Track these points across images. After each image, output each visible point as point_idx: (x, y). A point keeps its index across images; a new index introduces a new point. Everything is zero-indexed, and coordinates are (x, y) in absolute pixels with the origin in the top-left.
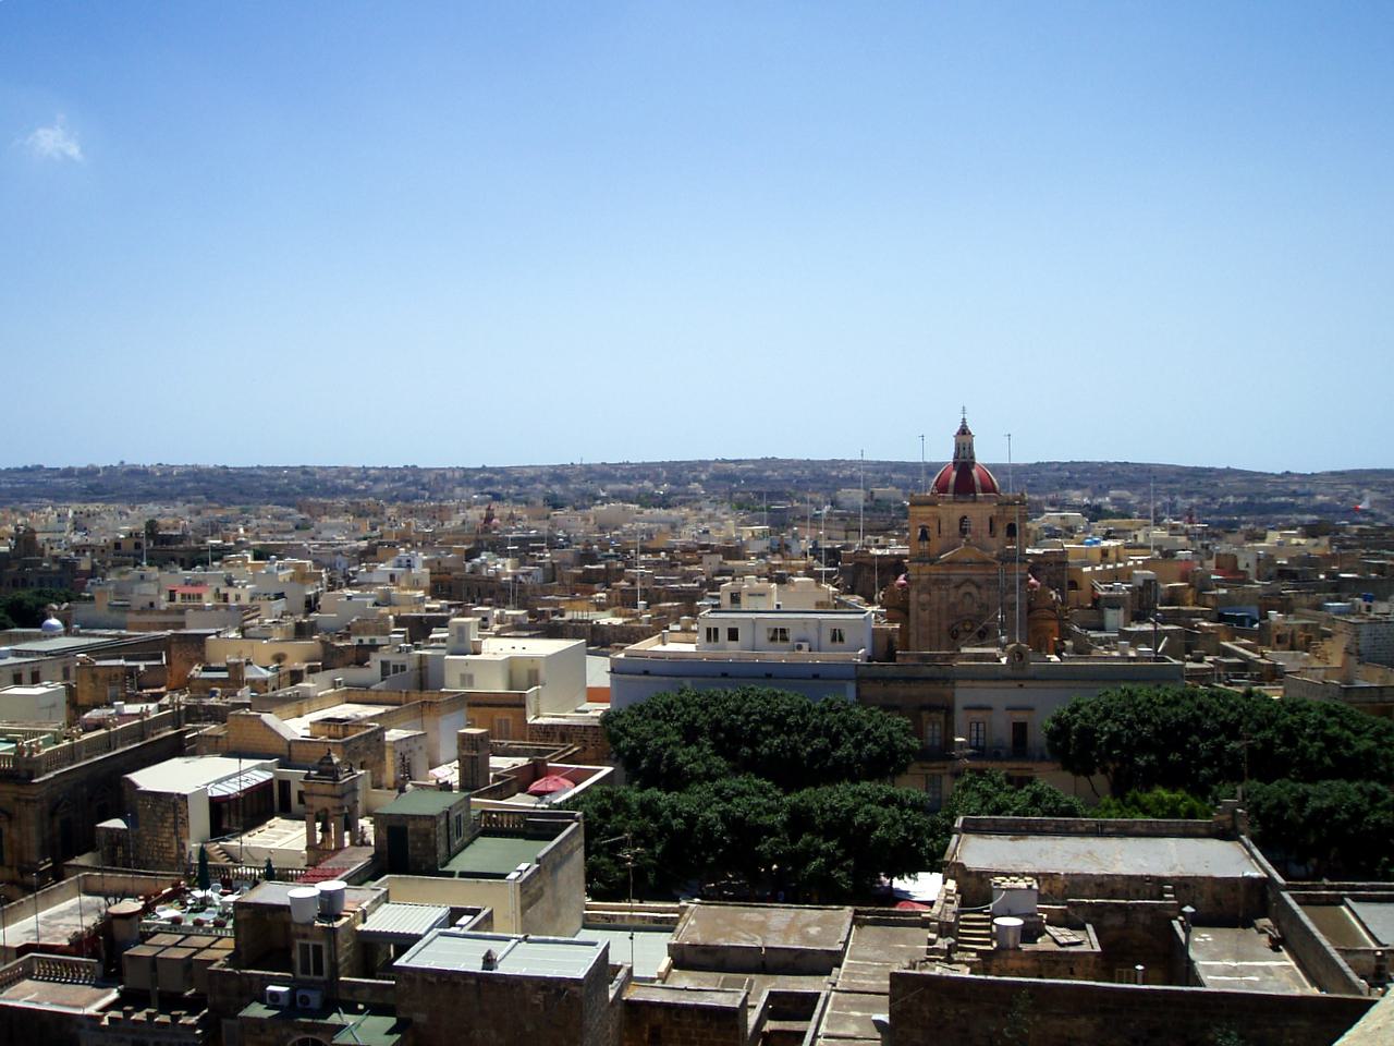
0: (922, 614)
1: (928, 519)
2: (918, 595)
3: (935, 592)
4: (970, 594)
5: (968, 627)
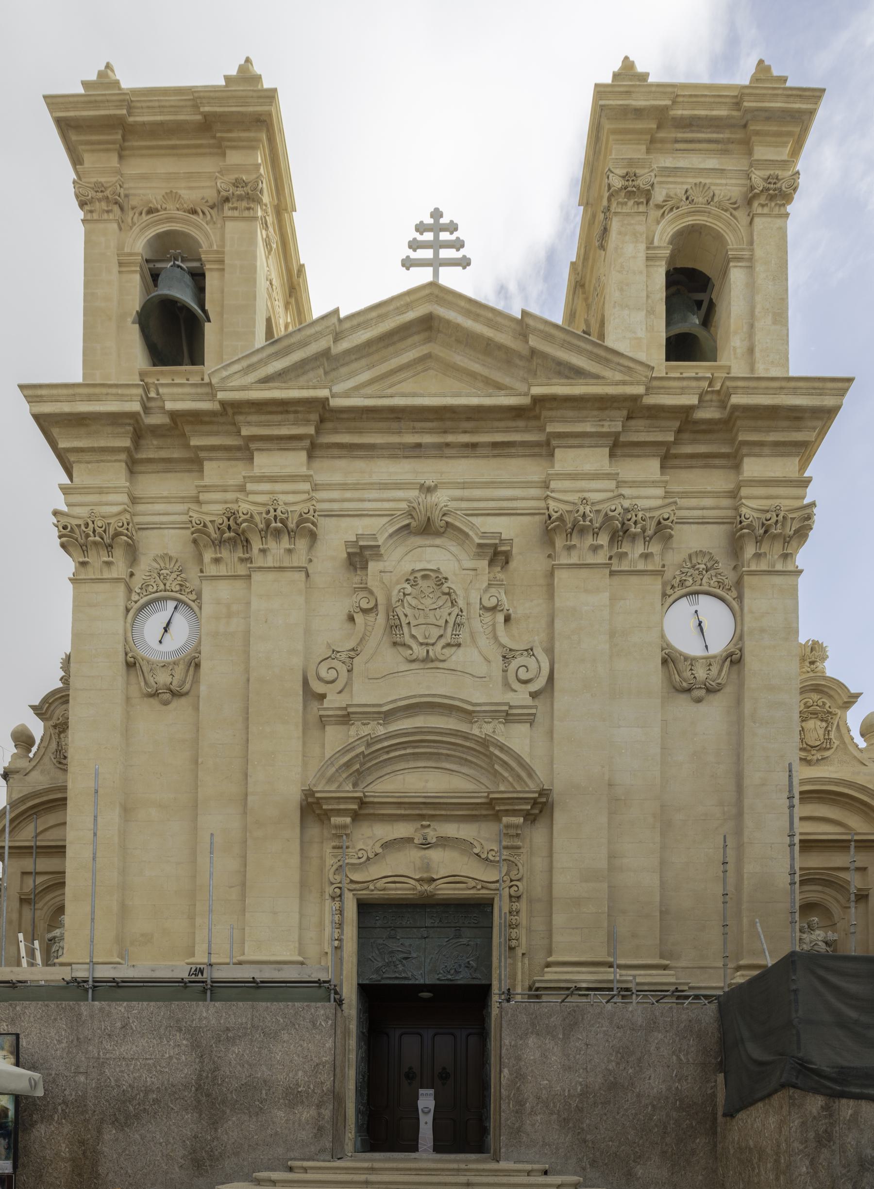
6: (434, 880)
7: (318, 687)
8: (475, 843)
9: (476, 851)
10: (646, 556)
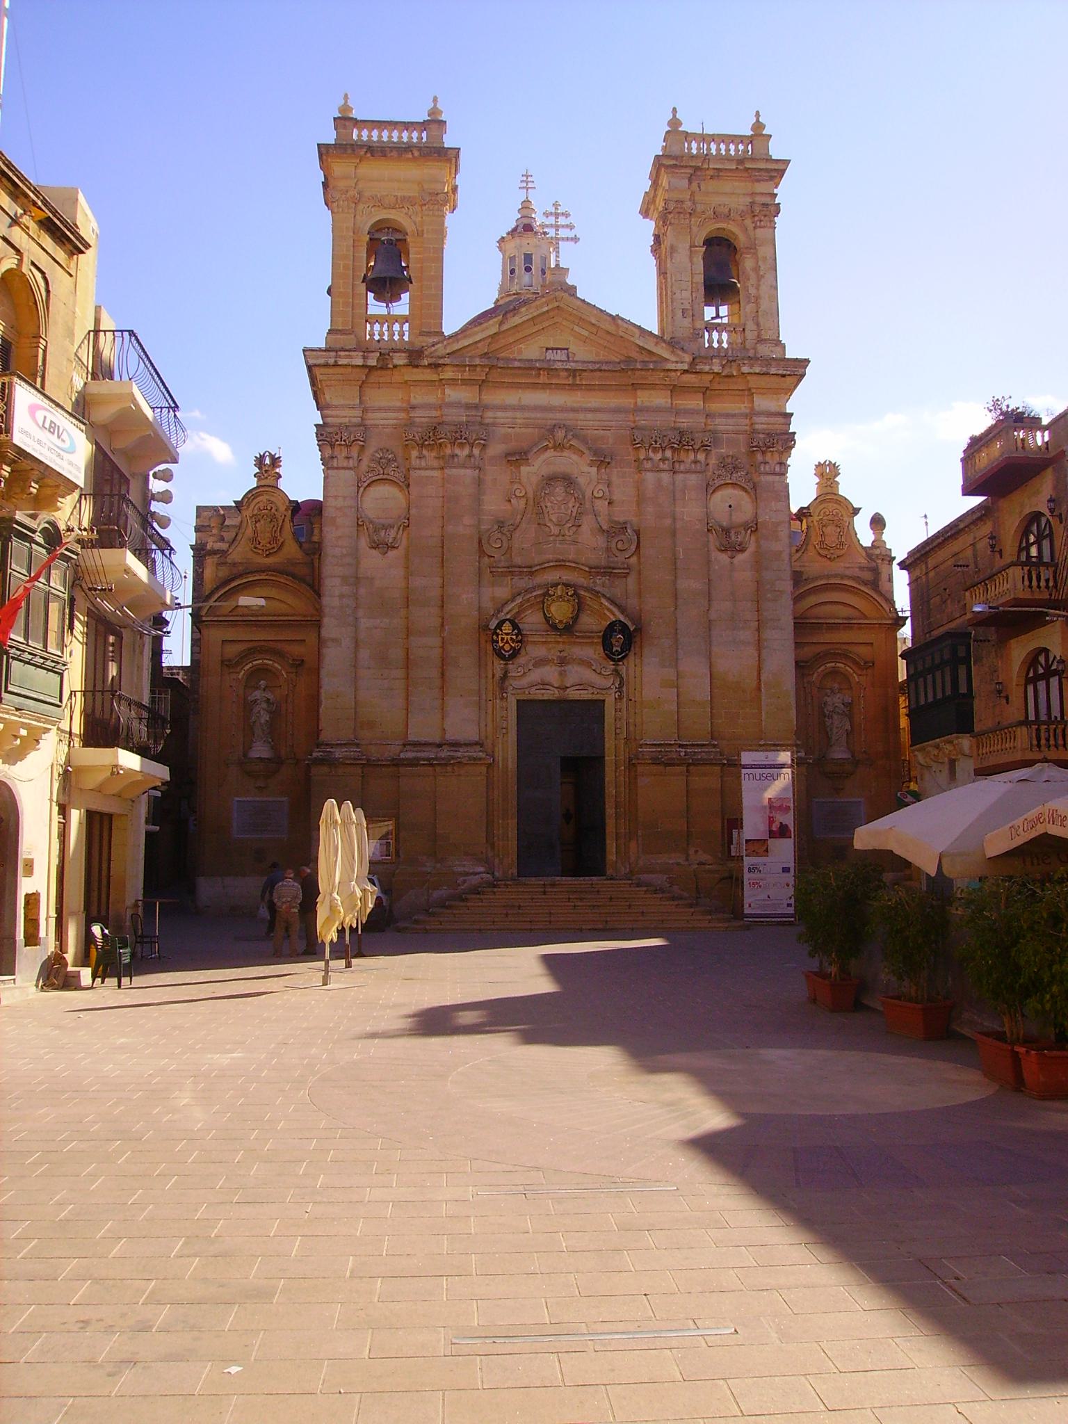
0: (372, 561)
1: (401, 203)
2: (363, 485)
3: (425, 467)
4: (568, 481)
5: (560, 611)
7: (490, 552)
9: (594, 668)
10: (696, 462)
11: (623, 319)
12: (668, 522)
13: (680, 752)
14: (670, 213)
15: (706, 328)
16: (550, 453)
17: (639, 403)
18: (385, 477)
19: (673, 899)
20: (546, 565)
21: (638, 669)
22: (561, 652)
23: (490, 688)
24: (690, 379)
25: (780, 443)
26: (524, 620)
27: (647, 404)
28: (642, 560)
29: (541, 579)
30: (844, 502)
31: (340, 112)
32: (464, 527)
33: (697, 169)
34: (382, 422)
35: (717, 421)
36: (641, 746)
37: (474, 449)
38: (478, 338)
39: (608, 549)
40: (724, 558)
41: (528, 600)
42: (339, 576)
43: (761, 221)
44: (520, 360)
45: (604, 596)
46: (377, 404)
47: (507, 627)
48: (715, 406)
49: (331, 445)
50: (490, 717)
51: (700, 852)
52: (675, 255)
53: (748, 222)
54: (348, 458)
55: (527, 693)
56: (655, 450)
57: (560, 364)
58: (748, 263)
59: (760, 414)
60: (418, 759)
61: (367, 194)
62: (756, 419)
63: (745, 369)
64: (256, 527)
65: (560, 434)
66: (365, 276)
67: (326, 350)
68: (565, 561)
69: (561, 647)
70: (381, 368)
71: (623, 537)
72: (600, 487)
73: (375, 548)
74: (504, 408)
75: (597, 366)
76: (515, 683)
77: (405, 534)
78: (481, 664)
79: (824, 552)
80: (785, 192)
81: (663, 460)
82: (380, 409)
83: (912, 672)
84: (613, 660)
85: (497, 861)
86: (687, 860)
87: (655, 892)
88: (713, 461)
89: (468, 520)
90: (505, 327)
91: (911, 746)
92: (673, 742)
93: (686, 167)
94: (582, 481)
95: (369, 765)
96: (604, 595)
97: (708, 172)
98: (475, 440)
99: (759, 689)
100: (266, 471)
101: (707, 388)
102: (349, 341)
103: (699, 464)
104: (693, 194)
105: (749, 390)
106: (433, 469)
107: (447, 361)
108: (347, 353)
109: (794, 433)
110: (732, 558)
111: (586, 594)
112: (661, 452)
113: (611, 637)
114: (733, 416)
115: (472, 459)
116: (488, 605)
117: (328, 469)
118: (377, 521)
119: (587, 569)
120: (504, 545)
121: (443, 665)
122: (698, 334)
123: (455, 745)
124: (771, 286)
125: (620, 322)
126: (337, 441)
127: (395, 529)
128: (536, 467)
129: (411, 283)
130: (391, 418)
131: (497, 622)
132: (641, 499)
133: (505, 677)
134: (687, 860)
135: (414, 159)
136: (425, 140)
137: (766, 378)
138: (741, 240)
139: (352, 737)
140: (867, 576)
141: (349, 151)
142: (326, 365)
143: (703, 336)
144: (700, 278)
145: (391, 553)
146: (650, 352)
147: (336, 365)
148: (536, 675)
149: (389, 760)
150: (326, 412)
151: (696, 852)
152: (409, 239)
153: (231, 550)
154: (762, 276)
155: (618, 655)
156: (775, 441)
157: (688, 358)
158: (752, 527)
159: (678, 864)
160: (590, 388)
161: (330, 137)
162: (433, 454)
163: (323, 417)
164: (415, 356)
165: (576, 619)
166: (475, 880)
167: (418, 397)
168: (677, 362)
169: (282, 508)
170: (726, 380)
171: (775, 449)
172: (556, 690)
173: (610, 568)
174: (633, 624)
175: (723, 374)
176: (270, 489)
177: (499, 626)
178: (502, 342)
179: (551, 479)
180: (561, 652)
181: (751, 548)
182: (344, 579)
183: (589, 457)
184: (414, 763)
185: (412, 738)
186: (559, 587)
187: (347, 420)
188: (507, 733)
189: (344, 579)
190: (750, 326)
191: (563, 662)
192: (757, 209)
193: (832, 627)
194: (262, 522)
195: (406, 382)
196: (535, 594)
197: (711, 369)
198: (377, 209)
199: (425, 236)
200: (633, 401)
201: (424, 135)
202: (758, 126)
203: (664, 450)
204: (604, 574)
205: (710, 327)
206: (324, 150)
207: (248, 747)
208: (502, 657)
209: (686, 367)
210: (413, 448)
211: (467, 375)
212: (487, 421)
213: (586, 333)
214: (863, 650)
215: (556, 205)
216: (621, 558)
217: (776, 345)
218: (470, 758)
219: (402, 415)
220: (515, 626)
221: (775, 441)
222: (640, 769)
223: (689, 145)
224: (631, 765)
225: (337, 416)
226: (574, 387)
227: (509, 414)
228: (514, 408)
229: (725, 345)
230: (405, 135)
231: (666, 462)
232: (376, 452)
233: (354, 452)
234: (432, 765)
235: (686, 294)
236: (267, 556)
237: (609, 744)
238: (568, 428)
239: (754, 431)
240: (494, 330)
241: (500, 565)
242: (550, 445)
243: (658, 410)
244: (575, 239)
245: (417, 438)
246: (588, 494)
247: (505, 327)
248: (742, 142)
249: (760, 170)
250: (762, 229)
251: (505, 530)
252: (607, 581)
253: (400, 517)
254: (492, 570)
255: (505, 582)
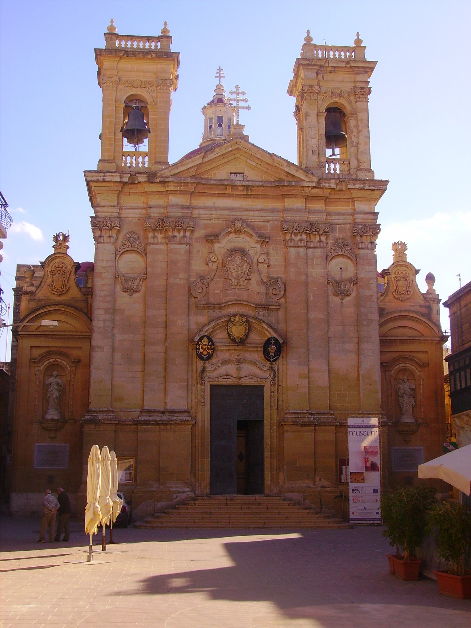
0: (124, 299)
1: (143, 85)
2: (119, 253)
4: (243, 252)
5: (237, 331)
6: (241, 378)
8: (257, 362)
9: (258, 366)
10: (320, 242)
11: (277, 156)
12: (303, 277)
13: (310, 417)
14: (305, 93)
15: (327, 161)
16: (232, 236)
17: (286, 205)
18: (132, 249)
19: (306, 509)
20: (229, 303)
21: (285, 367)
22: (238, 356)
23: (194, 377)
24: (316, 191)
25: (371, 230)
26: (217, 336)
27: (291, 207)
28: (288, 300)
29: (225, 312)
30: (409, 266)
31: (108, 30)
32: (180, 279)
33: (322, 66)
34: (131, 216)
35: (334, 217)
36: (286, 414)
37: (186, 233)
38: (190, 166)
39: (267, 294)
40: (337, 299)
41: (218, 324)
42: (103, 309)
43: (359, 98)
44: (215, 180)
45: (264, 322)
46: (128, 205)
47: (205, 341)
48: (332, 208)
49: (100, 229)
50: (194, 396)
51: (322, 480)
52: (308, 117)
53: (352, 98)
54: (110, 237)
55: (217, 380)
56: (296, 234)
57: (239, 182)
58: (352, 123)
59: (360, 213)
60: (149, 421)
61: (124, 79)
62: (357, 216)
63: (350, 186)
64: (53, 278)
65: (238, 224)
66: (122, 128)
67: (98, 172)
68: (241, 301)
69: (238, 353)
70: (131, 183)
71: (276, 287)
72: (262, 256)
73: (125, 292)
74: (205, 208)
75: (261, 184)
76: (210, 375)
77: (144, 284)
78: (189, 363)
79: (397, 297)
80: (374, 81)
81: (301, 240)
82: (130, 208)
83: (452, 369)
84: (269, 361)
85: (197, 484)
86: (314, 484)
87: (294, 504)
88: (331, 241)
89: (182, 275)
90: (206, 160)
91: (452, 415)
92: (306, 412)
93: (315, 65)
94: (251, 252)
95: (119, 424)
96: (264, 322)
97: (328, 69)
98: (187, 227)
99: (359, 380)
100: (60, 244)
101: (327, 197)
102: (112, 167)
103: (322, 243)
104: (319, 81)
105: (353, 198)
106: (161, 244)
107: (171, 180)
108: (111, 174)
109: (380, 225)
110: (342, 299)
111: (254, 321)
112: (299, 236)
113: (268, 347)
114: (343, 214)
115: (185, 239)
116: (193, 326)
117: (98, 243)
118: (127, 275)
119: (254, 306)
120: (204, 291)
121: (166, 363)
122: (322, 165)
123: (173, 412)
124: (366, 137)
125: (275, 157)
126: (104, 226)
127: (138, 280)
128: (224, 244)
129: (150, 133)
130: (137, 213)
131: (199, 337)
132: (287, 264)
133: (203, 371)
134: (314, 484)
135: (152, 59)
136: (159, 47)
137: (363, 192)
138: (348, 109)
139: (110, 407)
140: (424, 311)
141: (114, 53)
142: (98, 181)
143: (325, 166)
144: (323, 132)
145: (136, 295)
146: (293, 176)
147: (104, 181)
148: (223, 370)
149: (132, 421)
150: (97, 209)
151: (320, 479)
152: (149, 107)
153: (37, 292)
154: (360, 131)
155: (272, 358)
156: (368, 229)
157: (315, 179)
158: (354, 281)
159: (309, 487)
160: (257, 197)
161: (102, 45)
162: (162, 235)
163: (95, 212)
164: (151, 176)
165: (247, 336)
166: (183, 496)
167: (154, 201)
168: (309, 181)
169: (69, 267)
170: (338, 192)
171: (368, 234)
172: (235, 379)
173: (268, 305)
174: (282, 339)
175: (337, 189)
176: (62, 255)
177: (201, 339)
178: (204, 169)
179: (233, 251)
180: (238, 356)
181: (354, 294)
182: (107, 310)
183: (255, 238)
184: (147, 423)
185: (146, 408)
186: (237, 316)
187: (109, 214)
188: (204, 405)
189: (107, 310)
190: (353, 160)
191: (239, 362)
192: (357, 91)
193: (403, 342)
194: (57, 275)
195: (146, 192)
196: (222, 320)
197: (329, 186)
198: (129, 88)
199: (158, 105)
200: (282, 205)
201: (159, 44)
202: (358, 41)
203: (301, 235)
204: (265, 309)
205: (329, 161)
206: (98, 53)
207: (45, 412)
208: (201, 358)
209: (314, 185)
210: (150, 231)
211: (182, 188)
212: (194, 216)
213: (254, 164)
214: (422, 357)
215: (237, 87)
216: (274, 299)
217: (369, 172)
218: (181, 420)
219: (144, 212)
220: (210, 340)
221: (368, 229)
222: (285, 428)
223: (317, 52)
224: (280, 425)
225: (104, 212)
226: (247, 196)
227: (208, 212)
228: (211, 208)
229: (338, 172)
230: (147, 44)
231: (302, 241)
232: (127, 233)
233: (114, 234)
234: (158, 424)
235: (315, 141)
236: (60, 295)
237: (267, 412)
238: (243, 221)
239: (356, 223)
240: (199, 161)
241: (202, 303)
242: (232, 231)
243: (298, 210)
244: (249, 108)
245: (152, 226)
246: (255, 260)
247: (206, 160)
248: (348, 51)
249: (359, 67)
250: (360, 103)
251: (205, 282)
252: (266, 313)
253: (140, 273)
254: (197, 306)
255: (204, 313)
